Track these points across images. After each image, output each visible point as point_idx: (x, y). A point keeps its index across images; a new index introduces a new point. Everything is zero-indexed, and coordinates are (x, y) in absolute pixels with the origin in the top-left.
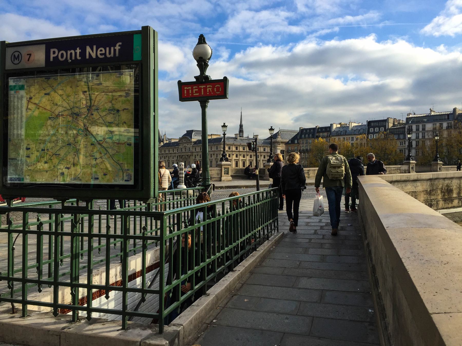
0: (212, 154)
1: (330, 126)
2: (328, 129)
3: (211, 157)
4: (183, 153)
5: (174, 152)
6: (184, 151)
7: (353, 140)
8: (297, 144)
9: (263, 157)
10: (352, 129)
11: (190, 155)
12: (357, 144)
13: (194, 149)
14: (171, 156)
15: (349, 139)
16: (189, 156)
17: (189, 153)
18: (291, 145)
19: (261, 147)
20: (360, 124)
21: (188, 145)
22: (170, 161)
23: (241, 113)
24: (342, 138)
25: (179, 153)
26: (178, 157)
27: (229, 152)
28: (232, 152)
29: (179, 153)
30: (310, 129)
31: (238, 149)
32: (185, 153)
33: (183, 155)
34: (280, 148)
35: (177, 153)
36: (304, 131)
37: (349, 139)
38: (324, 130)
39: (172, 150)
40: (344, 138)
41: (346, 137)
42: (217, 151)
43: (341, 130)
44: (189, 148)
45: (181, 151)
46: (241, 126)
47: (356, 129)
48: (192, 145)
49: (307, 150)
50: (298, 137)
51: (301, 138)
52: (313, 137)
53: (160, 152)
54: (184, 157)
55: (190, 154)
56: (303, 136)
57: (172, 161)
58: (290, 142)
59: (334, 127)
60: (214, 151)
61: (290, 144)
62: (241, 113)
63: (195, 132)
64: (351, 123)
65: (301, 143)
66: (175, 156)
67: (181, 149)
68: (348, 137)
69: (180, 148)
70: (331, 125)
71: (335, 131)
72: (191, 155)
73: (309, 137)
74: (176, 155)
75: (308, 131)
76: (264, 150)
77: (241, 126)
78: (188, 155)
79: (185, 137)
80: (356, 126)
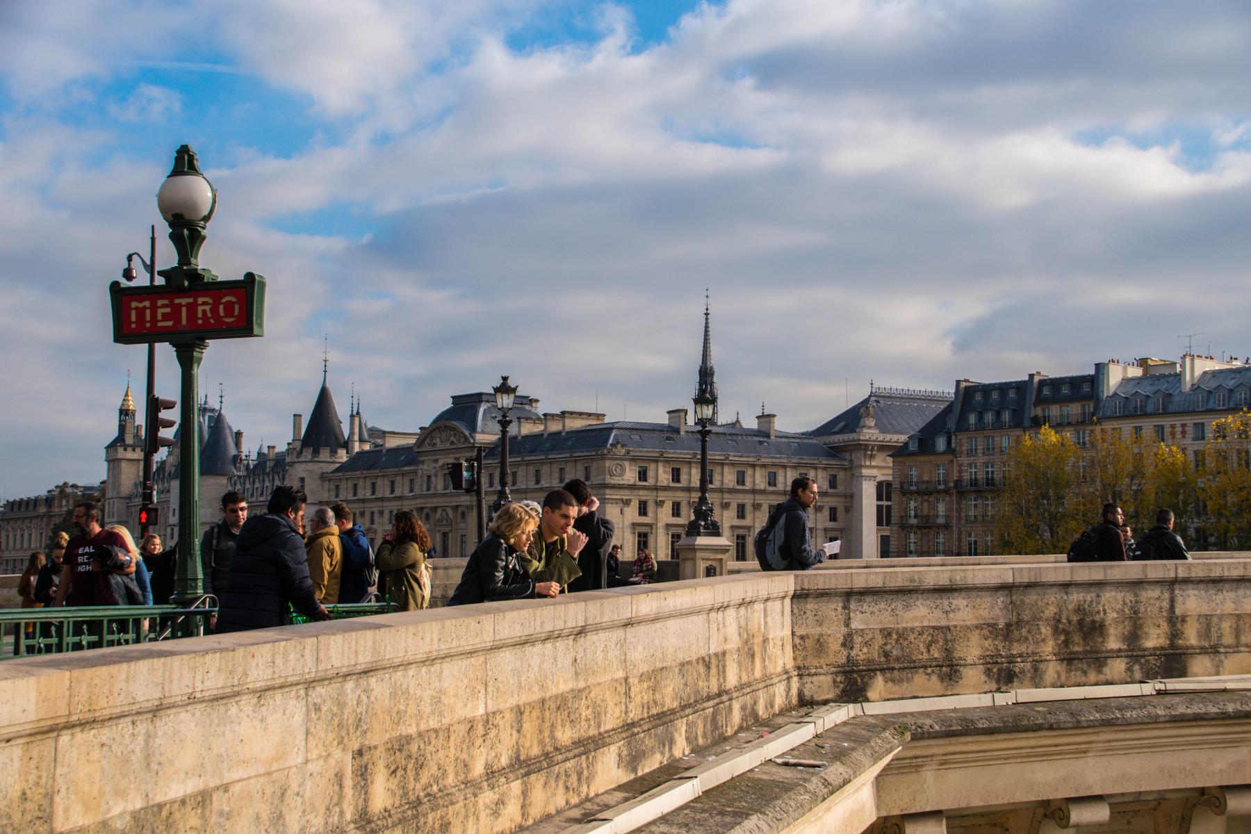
2: (1086, 388)
4: (434, 495)
5: (398, 493)
7: (1203, 438)
10: (1196, 388)
11: (467, 507)
12: (1222, 456)
14: (381, 513)
15: (1184, 433)
16: (463, 514)
18: (920, 458)
20: (1238, 364)
22: (376, 531)
23: (707, 314)
24: (1148, 426)
25: (415, 497)
27: (641, 492)
28: (655, 493)
29: (415, 497)
30: (1003, 388)
32: (441, 500)
34: (874, 472)
35: (408, 498)
36: (978, 397)
37: (1184, 433)
38: (1065, 390)
39: (387, 483)
40: (1160, 430)
41: (1166, 422)
43: (1146, 390)
45: (428, 489)
46: (706, 374)
47: (1213, 384)
49: (990, 482)
50: (951, 424)
51: (961, 426)
52: (1018, 423)
53: (333, 493)
54: (438, 515)
56: (972, 419)
58: (913, 447)
59: (1115, 377)
61: (913, 454)
62: (707, 314)
63: (489, 405)
64: (1192, 360)
65: (961, 452)
67: (429, 477)
68: (1178, 421)
71: (1115, 394)
73: (998, 425)
77: (706, 374)
78: (457, 507)
79: (447, 423)
80: (1215, 374)
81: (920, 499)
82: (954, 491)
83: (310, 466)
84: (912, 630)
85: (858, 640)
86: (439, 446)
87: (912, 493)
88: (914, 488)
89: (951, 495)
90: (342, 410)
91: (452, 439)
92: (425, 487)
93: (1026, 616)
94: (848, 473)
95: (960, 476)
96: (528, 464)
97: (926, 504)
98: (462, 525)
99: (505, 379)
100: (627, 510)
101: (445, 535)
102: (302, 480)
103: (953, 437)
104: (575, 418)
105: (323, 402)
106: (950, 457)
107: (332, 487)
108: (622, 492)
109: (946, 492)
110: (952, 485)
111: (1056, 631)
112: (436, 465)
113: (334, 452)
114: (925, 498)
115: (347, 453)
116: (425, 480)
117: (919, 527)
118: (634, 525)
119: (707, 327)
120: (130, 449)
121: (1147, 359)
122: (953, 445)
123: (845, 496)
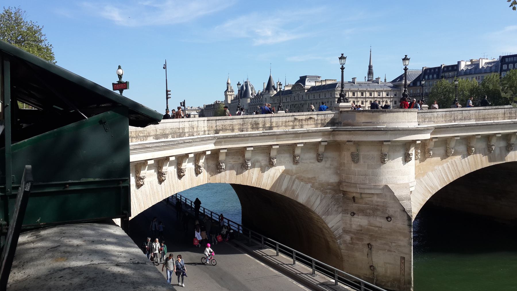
0: (326, 102)
1: (457, 64)
2: (455, 68)
6: (297, 99)
8: (419, 86)
11: (303, 104)
13: (308, 97)
15: (479, 79)
16: (303, 105)
18: (413, 88)
19: (392, 92)
21: (301, 92)
26: (292, 106)
30: (435, 69)
31: (356, 94)
32: (297, 102)
33: (296, 104)
35: (290, 102)
37: (479, 79)
42: (331, 98)
44: (303, 96)
46: (370, 67)
52: (438, 78)
53: (273, 102)
54: (297, 106)
55: (303, 102)
58: (411, 85)
60: (328, 98)
62: (371, 51)
63: (308, 78)
64: (482, 60)
66: (288, 105)
69: (293, 97)
70: (459, 63)
74: (290, 104)
75: (432, 71)
77: (370, 67)
78: (301, 104)
86: (296, 89)
89: (421, 97)
92: (294, 99)
94: (400, 92)
96: (317, 93)
98: (302, 108)
99: (239, 82)
102: (266, 98)
107: (273, 100)
109: (419, 96)
110: (421, 94)
112: (296, 94)
115: (276, 91)
116: (294, 97)
120: (229, 92)
121: (472, 59)
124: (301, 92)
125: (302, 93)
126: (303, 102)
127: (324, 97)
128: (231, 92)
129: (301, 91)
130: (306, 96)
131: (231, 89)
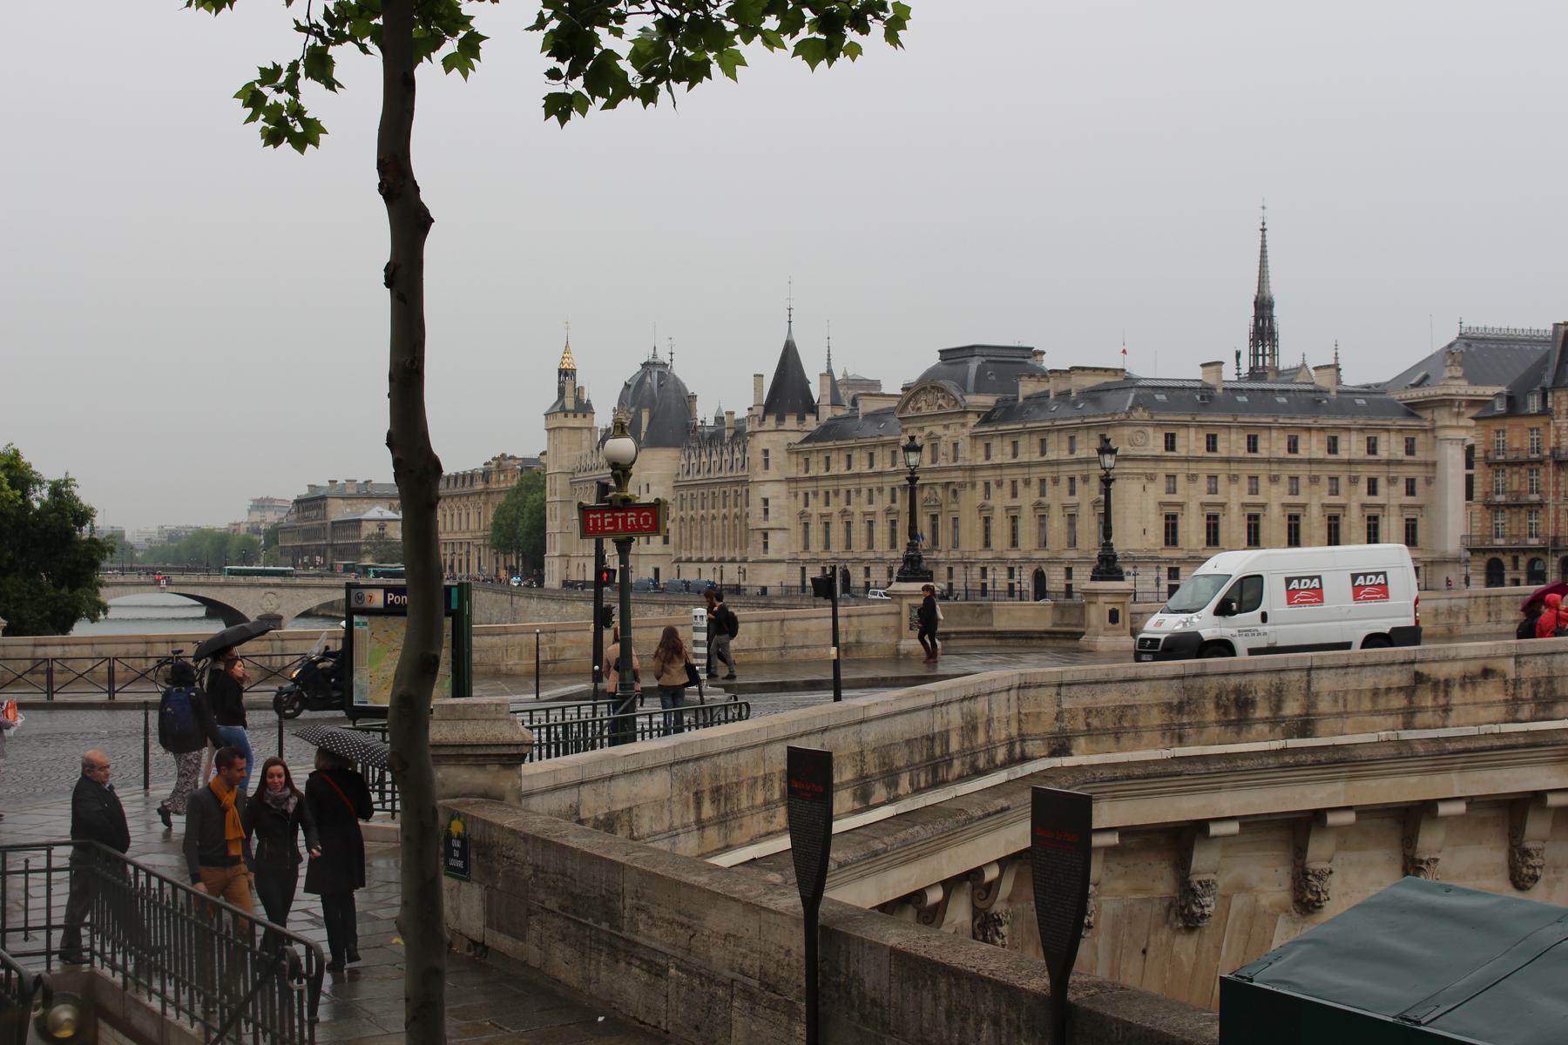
3: (1072, 493)
9: (1363, 487)
13: (981, 451)
16: (955, 492)
17: (954, 474)
23: (1263, 230)
27: (1170, 465)
39: (865, 455)
44: (956, 445)
46: (1263, 307)
48: (966, 431)
53: (802, 468)
55: (957, 477)
57: (865, 514)
58: (1500, 407)
62: (1263, 230)
65: (1559, 412)
66: (881, 490)
72: (963, 485)
76: (1372, 449)
77: (1263, 307)
81: (1508, 470)
82: (1551, 461)
83: (775, 436)
84: (1108, 708)
85: (1066, 715)
86: (925, 411)
87: (1498, 463)
88: (1501, 457)
90: (813, 370)
91: (940, 402)
93: (1195, 696)
94: (1430, 435)
95: (1558, 443)
96: (1031, 432)
97: (1516, 478)
98: (954, 507)
100: (1151, 487)
101: (934, 517)
102: (766, 452)
103: (1549, 394)
104: (1087, 375)
105: (790, 359)
106: (1545, 419)
107: (801, 460)
108: (1145, 465)
110: (1547, 453)
111: (1218, 706)
113: (801, 419)
114: (1515, 469)
117: (1508, 506)
118: (1162, 504)
119: (1263, 246)
122: (1550, 405)
123: (1426, 464)
124: (946, 427)
125: (950, 432)
126: (960, 473)
127: (1067, 452)
128: (580, 415)
129: (945, 423)
130: (973, 447)
131: (578, 400)
